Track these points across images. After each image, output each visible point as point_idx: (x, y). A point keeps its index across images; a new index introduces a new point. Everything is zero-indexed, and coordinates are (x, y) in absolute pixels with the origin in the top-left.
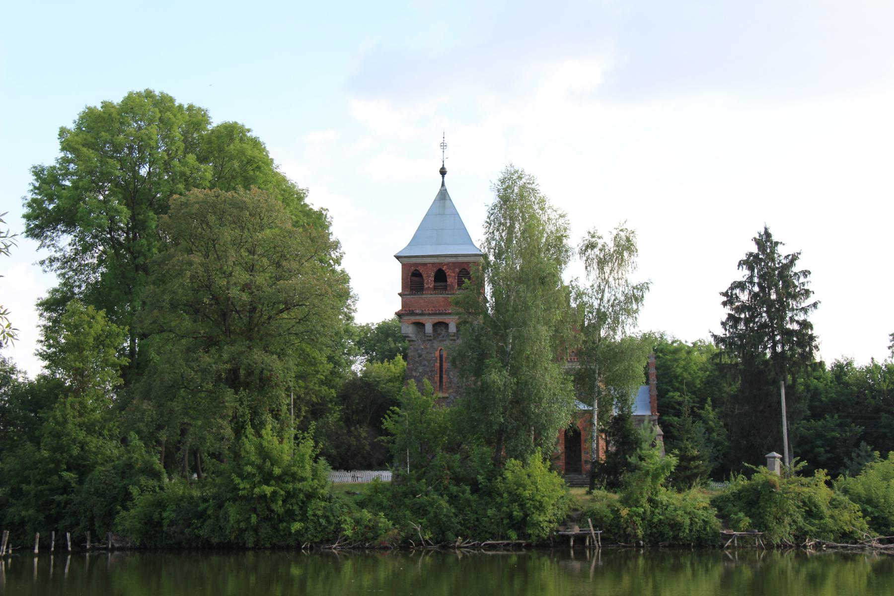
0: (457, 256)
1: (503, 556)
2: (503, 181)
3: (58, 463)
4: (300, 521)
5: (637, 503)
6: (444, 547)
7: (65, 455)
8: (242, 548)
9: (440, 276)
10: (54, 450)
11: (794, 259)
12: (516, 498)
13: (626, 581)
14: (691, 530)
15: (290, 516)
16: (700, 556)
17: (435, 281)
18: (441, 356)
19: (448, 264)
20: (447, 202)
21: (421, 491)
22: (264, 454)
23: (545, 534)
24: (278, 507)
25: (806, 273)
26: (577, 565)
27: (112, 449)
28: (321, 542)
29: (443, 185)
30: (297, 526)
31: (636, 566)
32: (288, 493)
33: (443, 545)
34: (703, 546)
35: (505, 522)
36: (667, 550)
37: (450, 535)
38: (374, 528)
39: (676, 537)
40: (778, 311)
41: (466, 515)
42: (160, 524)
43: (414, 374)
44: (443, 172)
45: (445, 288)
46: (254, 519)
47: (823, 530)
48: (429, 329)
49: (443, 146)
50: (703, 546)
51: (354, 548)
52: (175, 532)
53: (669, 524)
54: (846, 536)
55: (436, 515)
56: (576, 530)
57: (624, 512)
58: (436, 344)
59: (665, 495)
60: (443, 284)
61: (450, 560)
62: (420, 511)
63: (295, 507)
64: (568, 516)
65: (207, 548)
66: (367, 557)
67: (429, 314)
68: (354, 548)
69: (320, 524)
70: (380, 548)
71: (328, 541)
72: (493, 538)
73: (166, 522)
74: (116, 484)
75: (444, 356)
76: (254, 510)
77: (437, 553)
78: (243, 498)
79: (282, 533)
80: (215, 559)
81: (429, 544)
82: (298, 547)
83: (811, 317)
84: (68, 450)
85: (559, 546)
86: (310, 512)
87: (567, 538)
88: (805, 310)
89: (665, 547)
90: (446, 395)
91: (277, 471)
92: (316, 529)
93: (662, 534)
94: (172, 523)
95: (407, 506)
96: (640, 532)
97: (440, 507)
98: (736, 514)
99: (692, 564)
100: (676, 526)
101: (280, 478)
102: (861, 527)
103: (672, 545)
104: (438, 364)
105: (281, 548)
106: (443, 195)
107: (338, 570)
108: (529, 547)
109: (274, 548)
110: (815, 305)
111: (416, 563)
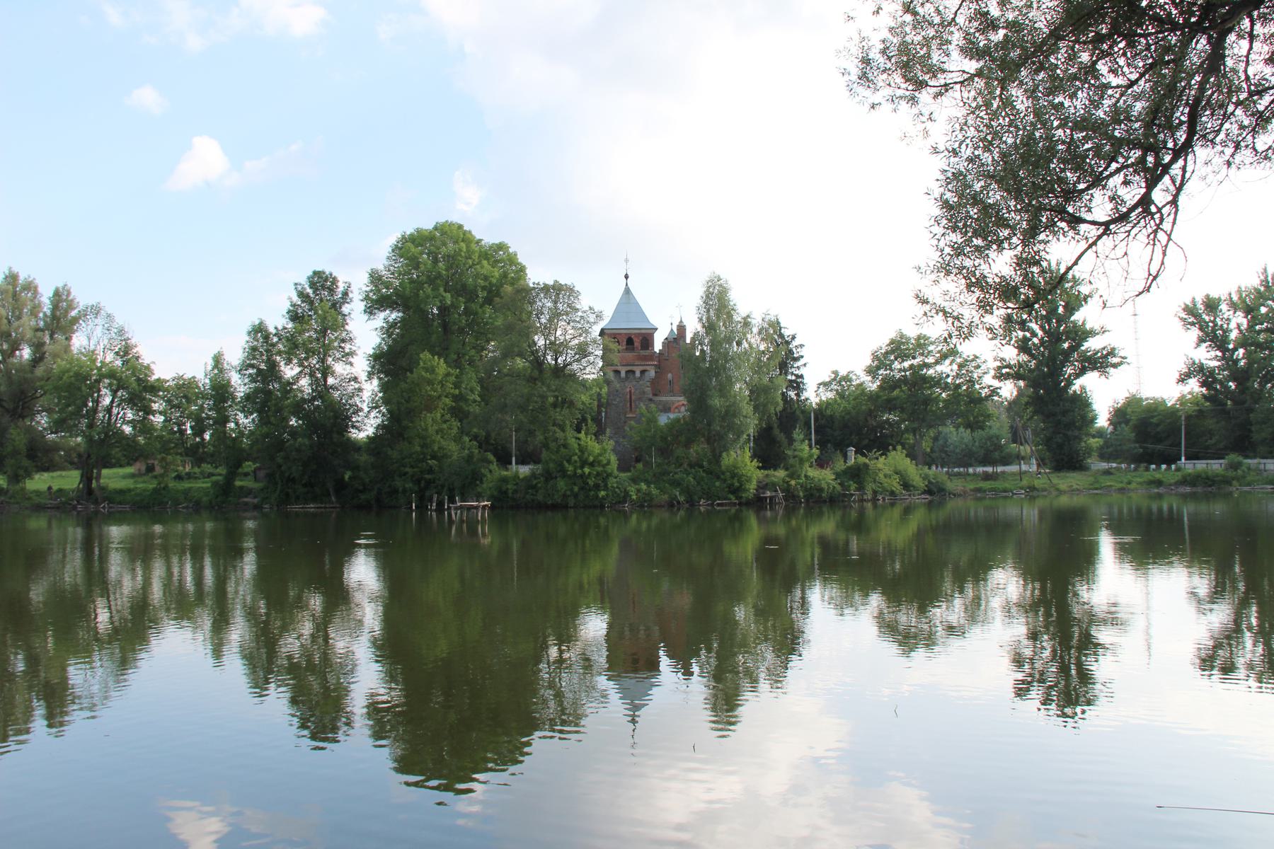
3: (423, 453)
5: (799, 477)
8: (565, 507)
9: (630, 341)
10: (422, 447)
11: (794, 338)
12: (734, 475)
13: (794, 522)
15: (597, 487)
22: (582, 450)
23: (751, 496)
24: (591, 482)
25: (802, 346)
26: (769, 513)
27: (453, 447)
30: (602, 493)
33: (692, 503)
34: (834, 501)
37: (696, 498)
38: (649, 494)
39: (820, 497)
40: (784, 367)
42: (506, 492)
44: (626, 277)
46: (576, 489)
47: (885, 490)
48: (623, 374)
49: (627, 261)
50: (834, 501)
54: (892, 493)
56: (768, 494)
57: (793, 482)
59: (814, 473)
62: (676, 484)
78: (570, 477)
80: (549, 514)
82: (602, 507)
83: (802, 371)
85: (759, 503)
91: (591, 459)
94: (515, 491)
96: (801, 494)
100: (821, 490)
101: (592, 465)
103: (816, 501)
106: (627, 291)
108: (740, 504)
109: (585, 507)
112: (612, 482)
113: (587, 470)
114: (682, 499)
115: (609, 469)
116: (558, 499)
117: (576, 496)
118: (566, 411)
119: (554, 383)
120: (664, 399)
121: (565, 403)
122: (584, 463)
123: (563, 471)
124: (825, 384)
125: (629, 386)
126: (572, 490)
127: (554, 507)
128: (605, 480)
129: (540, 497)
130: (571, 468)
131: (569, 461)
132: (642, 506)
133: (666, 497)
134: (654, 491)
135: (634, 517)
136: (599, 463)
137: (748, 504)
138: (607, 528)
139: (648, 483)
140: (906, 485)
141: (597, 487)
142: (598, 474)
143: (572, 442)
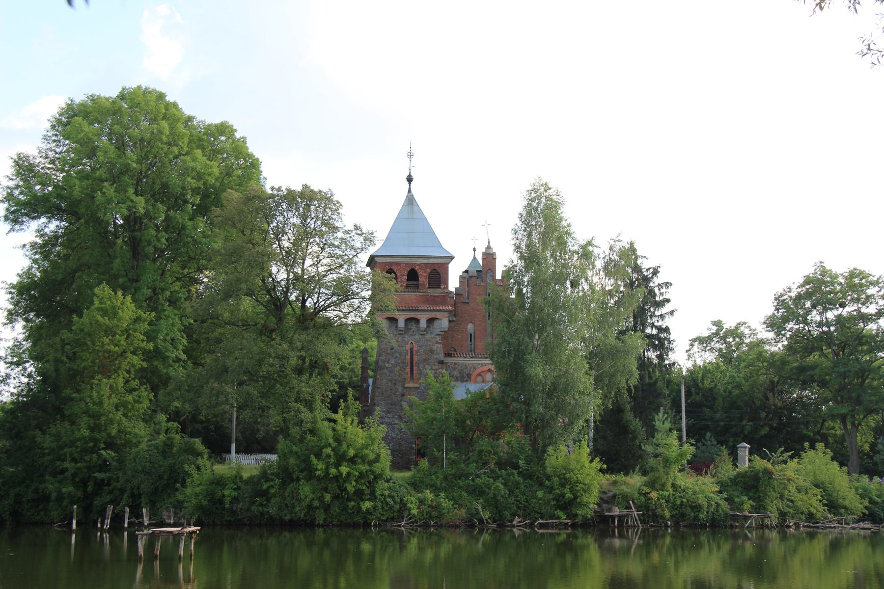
0: (429, 257)
1: (551, 534)
2: (530, 192)
3: (96, 441)
4: (369, 500)
5: (663, 486)
6: (499, 526)
7: (104, 434)
10: (92, 429)
11: (656, 272)
13: (656, 557)
14: (708, 512)
15: (359, 495)
16: (714, 534)
17: (408, 280)
18: (412, 350)
19: (420, 265)
20: (415, 208)
21: (471, 474)
23: (590, 514)
24: (350, 487)
25: (668, 285)
26: (617, 542)
27: (141, 430)
28: (387, 520)
29: (410, 191)
30: (367, 505)
31: (664, 543)
32: (361, 473)
33: (501, 524)
34: (718, 526)
35: (553, 503)
36: (685, 530)
37: (507, 514)
38: (437, 507)
39: (696, 518)
40: (640, 317)
41: (517, 496)
42: (221, 502)
43: (387, 365)
44: (410, 179)
45: (417, 286)
46: (328, 497)
48: (401, 324)
49: (410, 155)
51: (420, 526)
52: (241, 509)
53: (690, 506)
54: (811, 517)
55: (495, 496)
56: (616, 511)
57: (654, 495)
58: (407, 338)
60: (415, 283)
61: (507, 538)
62: (478, 492)
63: (364, 488)
64: (601, 499)
65: (275, 525)
66: (431, 534)
67: (403, 310)
68: (420, 526)
69: (387, 504)
70: (449, 526)
71: (393, 519)
72: (542, 518)
73: (227, 500)
74: (161, 463)
75: (415, 349)
76: (326, 490)
77: (494, 530)
78: (319, 479)
79: (350, 511)
80: (287, 534)
81: (489, 523)
82: (366, 525)
83: (667, 322)
84: (105, 430)
86: (379, 492)
87: (613, 517)
88: (662, 317)
89: (684, 526)
90: (417, 385)
91: (352, 452)
92: (383, 508)
93: (683, 515)
94: (235, 500)
95: (460, 487)
96: (667, 514)
97: (497, 488)
98: (738, 497)
99: (708, 541)
100: (697, 508)
101: (352, 461)
102: (819, 510)
103: (690, 525)
104: (409, 357)
105: (348, 526)
106: (410, 200)
107: (402, 548)
108: (574, 526)
109: (342, 525)
110: (672, 313)
111: (478, 541)
112: (382, 487)
113: (344, 470)
114: (486, 515)
115: (377, 468)
116: (300, 512)
117: (327, 508)
118: (316, 380)
119: (299, 338)
120: (460, 361)
121: (315, 366)
122: (341, 458)
123: (309, 470)
124: (703, 341)
125: (411, 341)
126: (321, 499)
127: (293, 525)
128: (371, 485)
129: (273, 510)
130: (321, 466)
131: (318, 456)
132: (426, 526)
133: (463, 512)
134: (446, 504)
135: (414, 541)
136: (364, 459)
137: (586, 525)
138: (372, 558)
139: (436, 490)
140: (833, 506)
141: (359, 495)
142: (362, 475)
143: (325, 427)
